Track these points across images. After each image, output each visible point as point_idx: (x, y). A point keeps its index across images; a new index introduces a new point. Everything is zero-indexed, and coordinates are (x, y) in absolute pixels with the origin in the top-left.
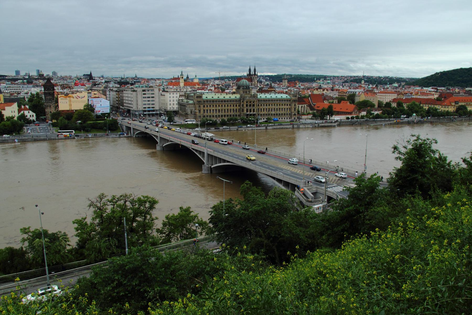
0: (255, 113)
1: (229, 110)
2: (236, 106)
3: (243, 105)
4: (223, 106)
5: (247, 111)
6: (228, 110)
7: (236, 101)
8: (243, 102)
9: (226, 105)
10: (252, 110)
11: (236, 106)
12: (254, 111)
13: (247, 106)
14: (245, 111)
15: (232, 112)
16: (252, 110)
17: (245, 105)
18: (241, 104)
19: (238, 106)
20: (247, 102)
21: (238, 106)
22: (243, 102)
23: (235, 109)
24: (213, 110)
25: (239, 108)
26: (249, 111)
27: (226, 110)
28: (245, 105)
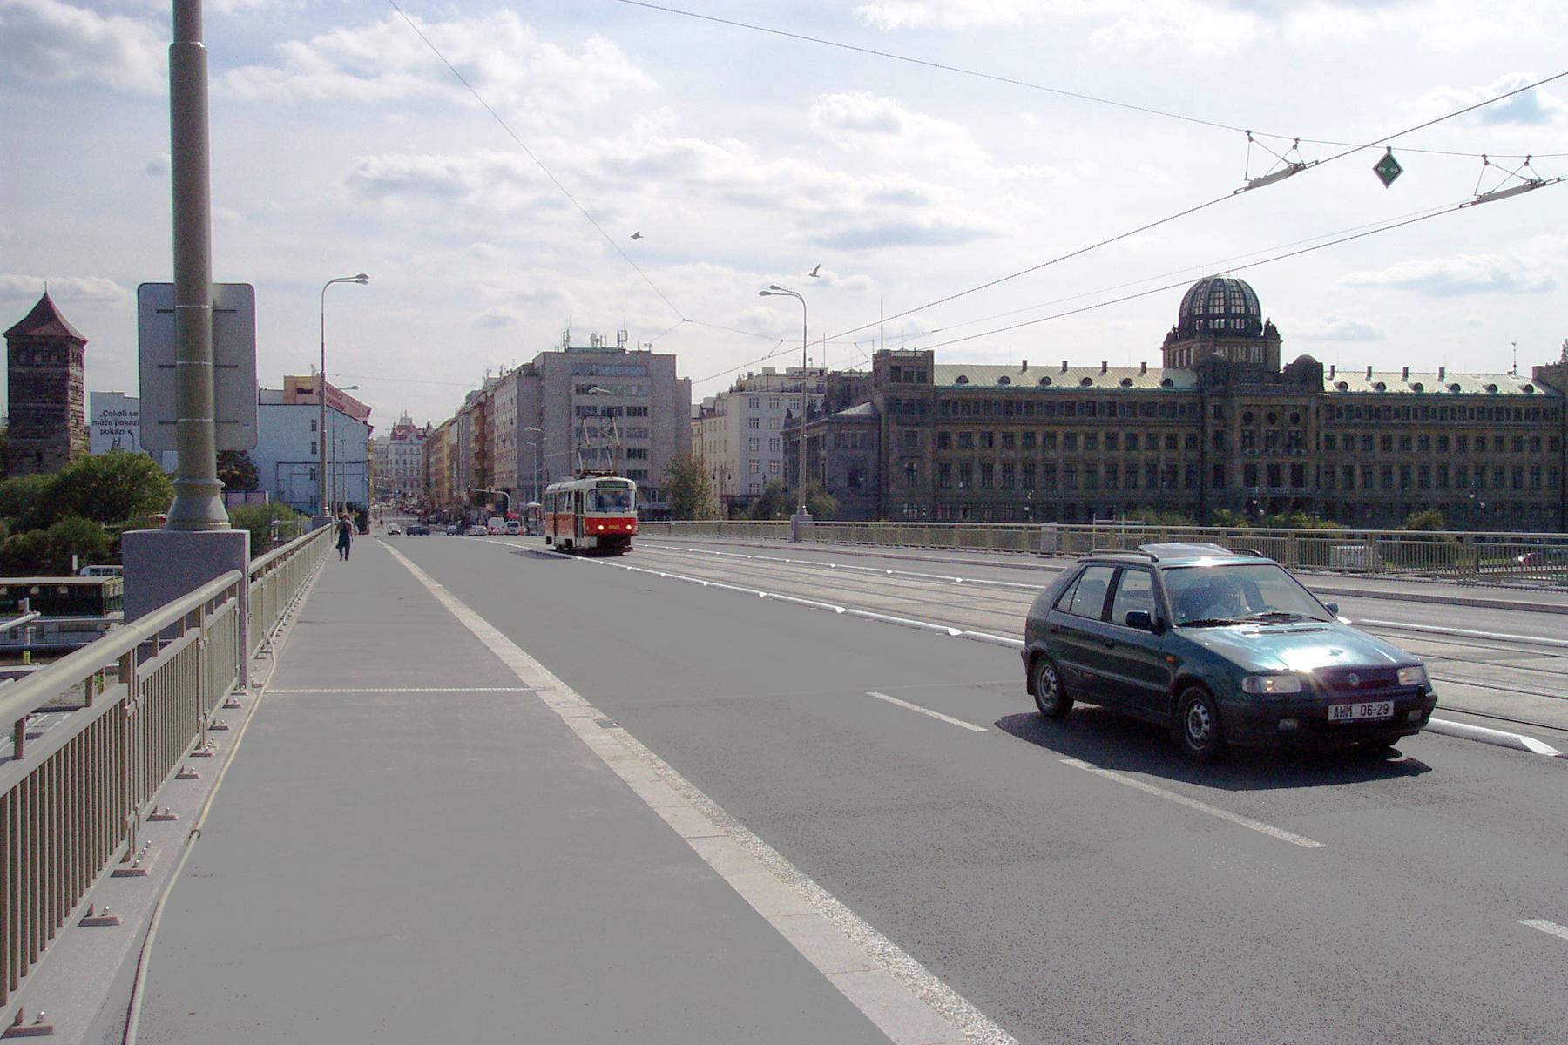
0: (1305, 491)
1: (1122, 468)
2: (1172, 442)
3: (1219, 437)
4: (1081, 439)
5: (1251, 474)
6: (1112, 470)
7: (1173, 406)
8: (1219, 413)
9: (1101, 437)
10: (1286, 473)
11: (1172, 442)
12: (1298, 480)
13: (1248, 440)
14: (1238, 479)
15: (1142, 481)
16: (1286, 473)
17: (1235, 437)
18: (1203, 429)
19: (1182, 443)
20: (1248, 418)
21: (1182, 443)
22: (1219, 413)
23: (1162, 466)
24: (1008, 468)
25: (1193, 455)
26: (1263, 476)
27: (1101, 470)
28: (1235, 437)
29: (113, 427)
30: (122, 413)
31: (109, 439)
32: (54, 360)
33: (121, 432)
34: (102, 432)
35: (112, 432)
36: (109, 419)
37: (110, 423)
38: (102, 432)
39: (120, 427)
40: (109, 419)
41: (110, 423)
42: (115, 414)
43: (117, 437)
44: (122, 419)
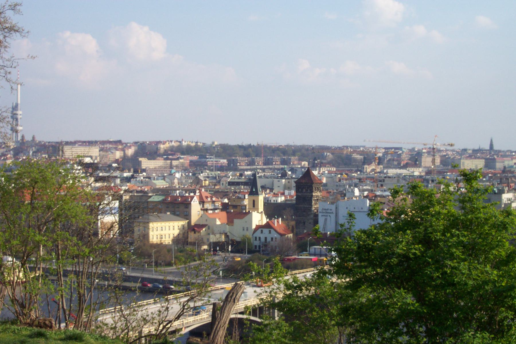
29: (325, 214)
30: (328, 209)
31: (324, 218)
32: (309, 191)
33: (326, 216)
34: (322, 216)
35: (324, 216)
36: (324, 211)
37: (324, 213)
38: (322, 216)
39: (327, 214)
40: (324, 211)
41: (324, 213)
42: (325, 210)
43: (326, 217)
44: (328, 211)
